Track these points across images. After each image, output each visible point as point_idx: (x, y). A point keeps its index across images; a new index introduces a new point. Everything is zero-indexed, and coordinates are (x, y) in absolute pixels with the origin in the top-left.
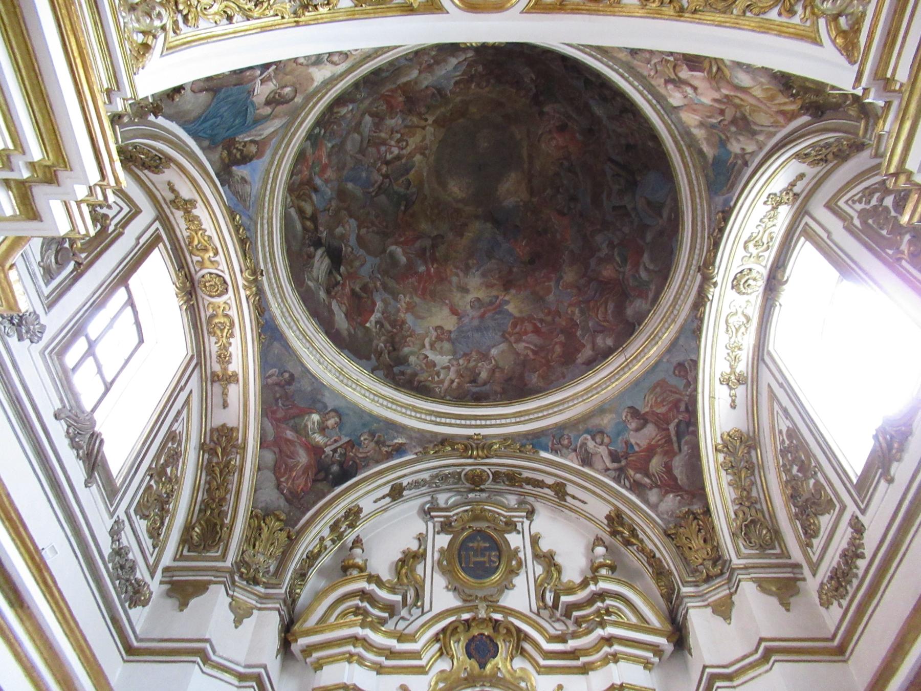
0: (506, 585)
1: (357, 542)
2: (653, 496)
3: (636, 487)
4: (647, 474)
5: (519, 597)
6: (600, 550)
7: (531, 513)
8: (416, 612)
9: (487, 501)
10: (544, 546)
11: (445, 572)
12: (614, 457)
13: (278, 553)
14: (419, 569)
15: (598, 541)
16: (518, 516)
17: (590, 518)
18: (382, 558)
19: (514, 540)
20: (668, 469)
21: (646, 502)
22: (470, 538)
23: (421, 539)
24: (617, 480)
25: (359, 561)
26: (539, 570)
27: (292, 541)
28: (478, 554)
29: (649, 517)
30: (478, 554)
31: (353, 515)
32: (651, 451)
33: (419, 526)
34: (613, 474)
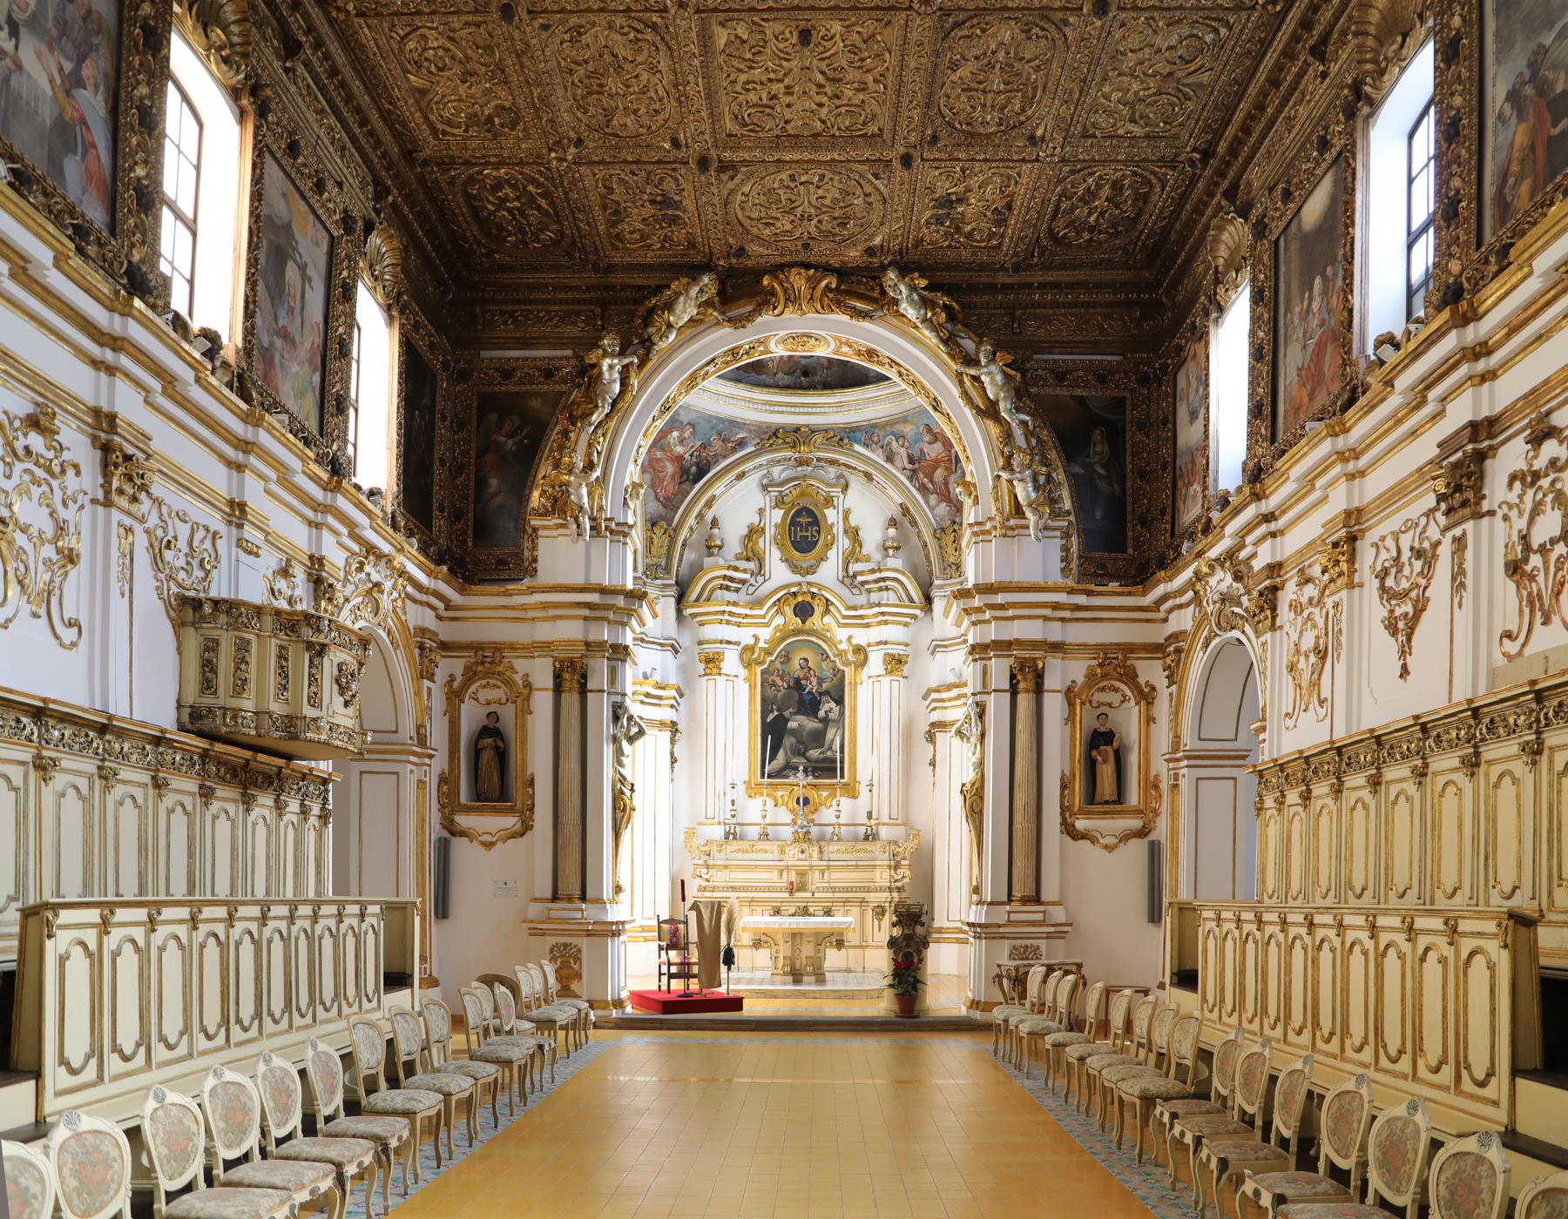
0: (822, 558)
1: (715, 523)
2: (933, 499)
3: (922, 489)
4: (931, 481)
5: (829, 572)
6: (892, 531)
7: (846, 487)
8: (760, 579)
9: (810, 477)
10: (853, 521)
11: (780, 546)
12: (911, 461)
13: (665, 550)
14: (761, 540)
15: (893, 522)
16: (836, 492)
17: (890, 498)
18: (732, 533)
19: (831, 515)
20: (946, 483)
21: (927, 503)
22: (798, 514)
23: (761, 512)
24: (910, 479)
25: (718, 542)
26: (847, 543)
27: (673, 540)
28: (804, 531)
29: (929, 512)
30: (804, 531)
31: (709, 504)
32: (937, 463)
33: (760, 500)
34: (908, 473)
